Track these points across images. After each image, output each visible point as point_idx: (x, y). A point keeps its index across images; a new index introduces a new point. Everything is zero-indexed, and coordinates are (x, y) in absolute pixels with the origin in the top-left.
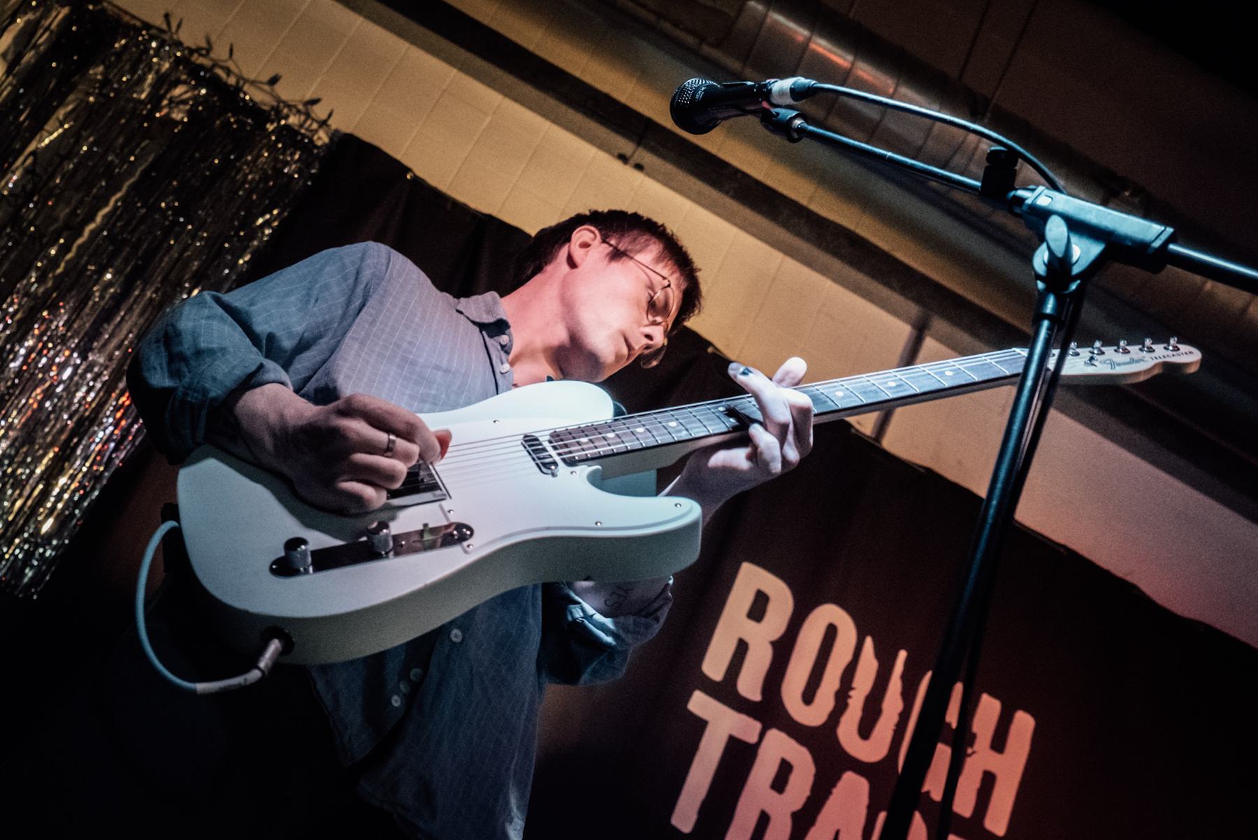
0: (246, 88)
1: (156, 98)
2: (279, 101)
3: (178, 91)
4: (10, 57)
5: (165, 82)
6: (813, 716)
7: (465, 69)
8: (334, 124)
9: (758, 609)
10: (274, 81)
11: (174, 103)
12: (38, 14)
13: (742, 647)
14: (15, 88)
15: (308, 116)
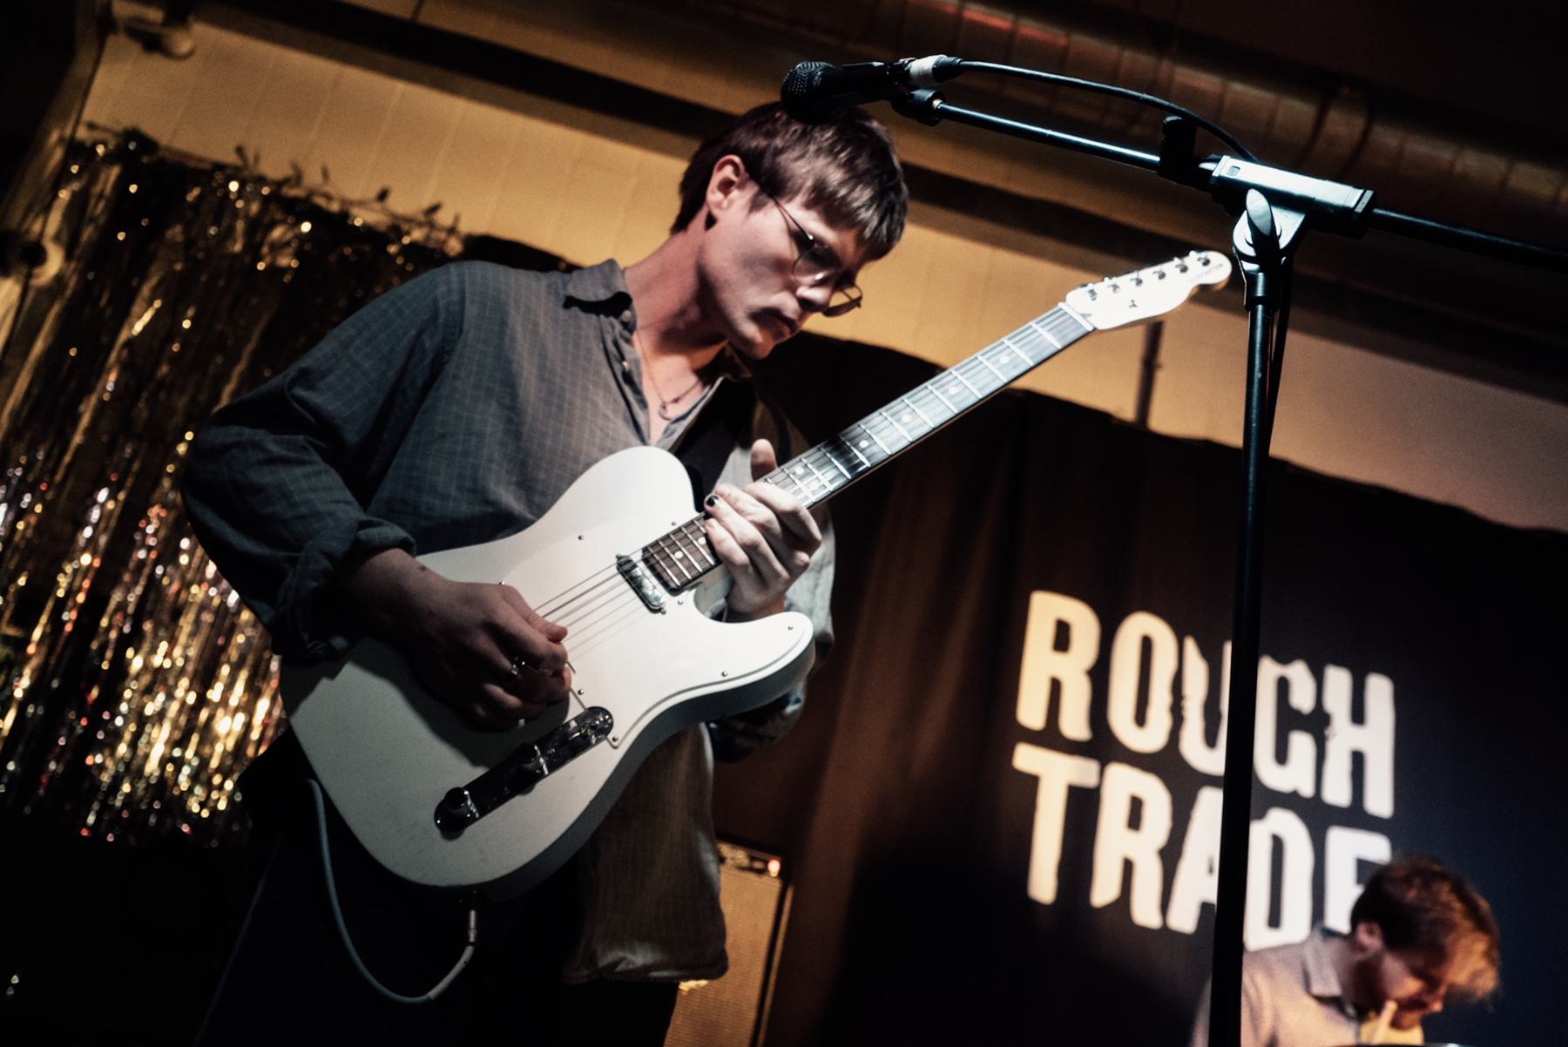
0: (355, 211)
1: (253, 250)
2: (394, 216)
3: (277, 233)
4: (65, 236)
5: (258, 228)
6: (1150, 739)
7: (593, 130)
8: (466, 227)
9: (1062, 638)
10: (383, 196)
11: (277, 248)
12: (83, 182)
13: (1056, 687)
14: (82, 275)
15: (432, 225)
